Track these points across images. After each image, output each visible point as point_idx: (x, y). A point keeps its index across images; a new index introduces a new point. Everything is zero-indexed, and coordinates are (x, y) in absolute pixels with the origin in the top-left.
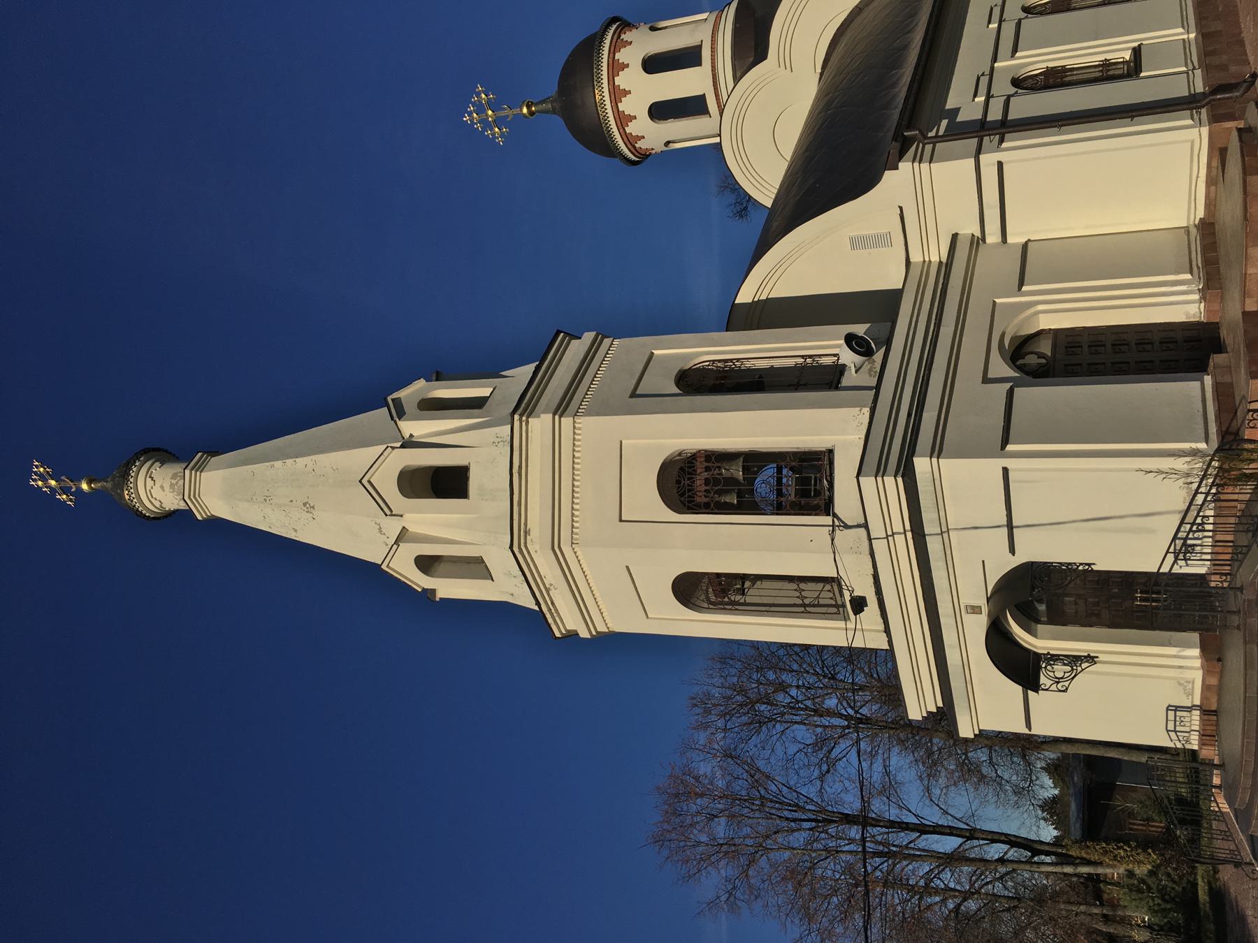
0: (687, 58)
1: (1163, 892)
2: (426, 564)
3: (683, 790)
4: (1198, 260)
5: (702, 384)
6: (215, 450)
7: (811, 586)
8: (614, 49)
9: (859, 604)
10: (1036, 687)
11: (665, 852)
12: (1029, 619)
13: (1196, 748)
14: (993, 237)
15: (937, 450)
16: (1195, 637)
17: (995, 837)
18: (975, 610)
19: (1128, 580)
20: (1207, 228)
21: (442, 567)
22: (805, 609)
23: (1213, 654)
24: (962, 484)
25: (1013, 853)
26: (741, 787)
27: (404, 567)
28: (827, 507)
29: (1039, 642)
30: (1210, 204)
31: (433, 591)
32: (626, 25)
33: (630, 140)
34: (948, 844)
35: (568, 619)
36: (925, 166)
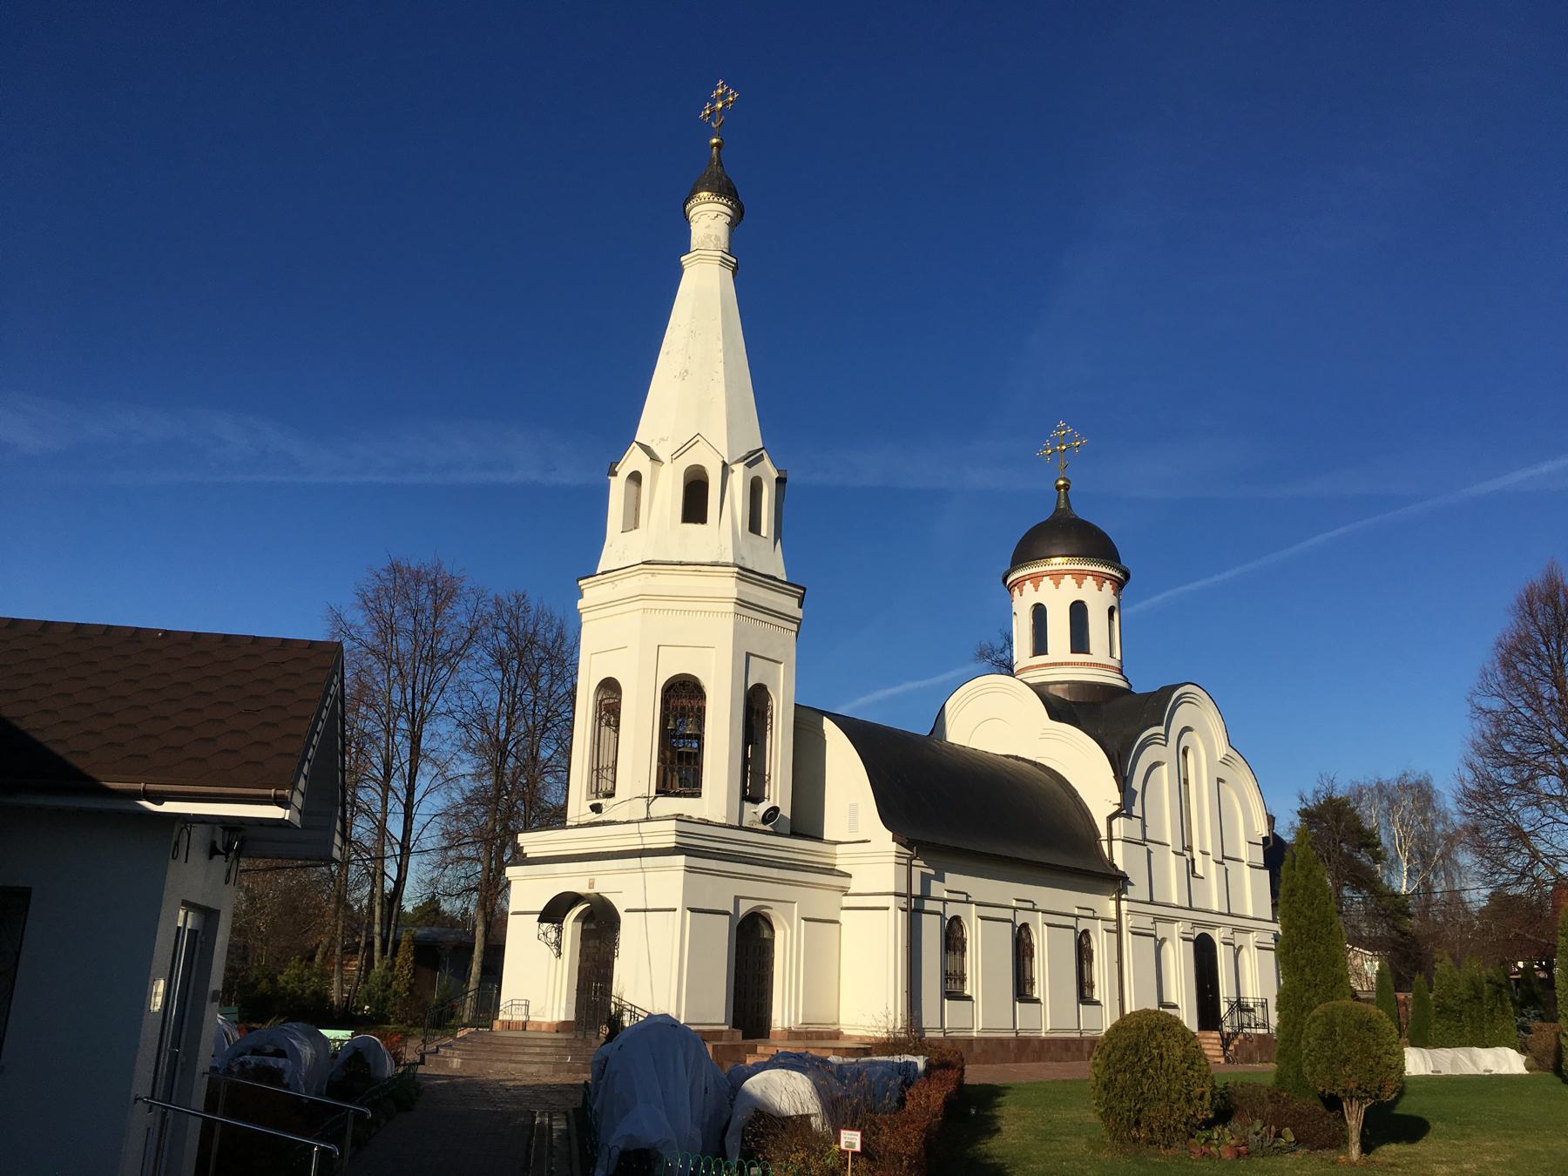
0: (1080, 642)
1: (386, 999)
2: (635, 477)
3: (444, 593)
4: (812, 1028)
5: (755, 705)
6: (735, 271)
7: (610, 777)
8: (1094, 575)
9: (596, 808)
10: (541, 920)
11: (384, 575)
12: (584, 918)
13: (502, 1017)
14: (847, 902)
15: (689, 869)
16: (572, 1018)
17: (402, 869)
18: (591, 885)
19: (608, 979)
20: (837, 1035)
21: (633, 487)
22: (597, 771)
23: (563, 1027)
24: (668, 881)
25: (389, 885)
26: (444, 644)
27: (633, 460)
28: (663, 791)
29: (571, 924)
30: (850, 1037)
31: (615, 474)
32: (1119, 585)
33: (1020, 583)
34: (395, 827)
35: (592, 593)
36: (893, 859)
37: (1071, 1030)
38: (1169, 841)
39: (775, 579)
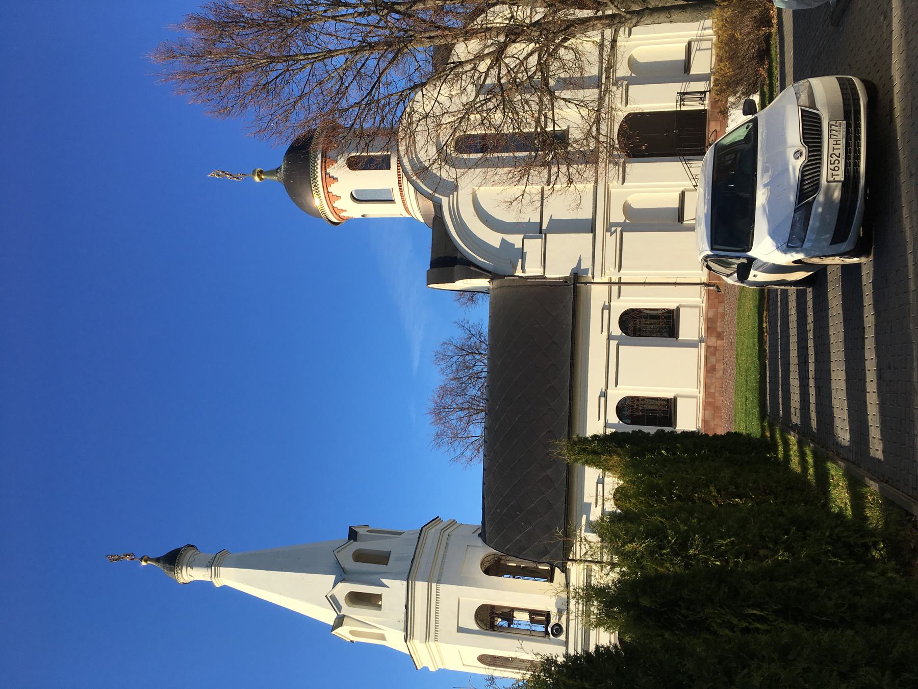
8: (326, 186)
37: (699, 356)
38: (539, 188)
39: (406, 607)
